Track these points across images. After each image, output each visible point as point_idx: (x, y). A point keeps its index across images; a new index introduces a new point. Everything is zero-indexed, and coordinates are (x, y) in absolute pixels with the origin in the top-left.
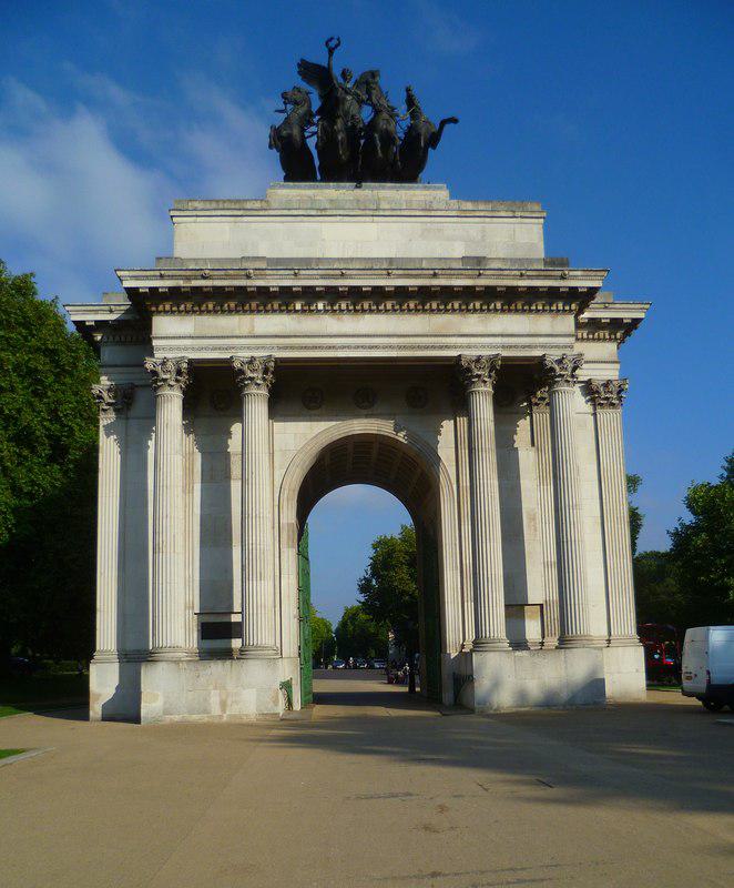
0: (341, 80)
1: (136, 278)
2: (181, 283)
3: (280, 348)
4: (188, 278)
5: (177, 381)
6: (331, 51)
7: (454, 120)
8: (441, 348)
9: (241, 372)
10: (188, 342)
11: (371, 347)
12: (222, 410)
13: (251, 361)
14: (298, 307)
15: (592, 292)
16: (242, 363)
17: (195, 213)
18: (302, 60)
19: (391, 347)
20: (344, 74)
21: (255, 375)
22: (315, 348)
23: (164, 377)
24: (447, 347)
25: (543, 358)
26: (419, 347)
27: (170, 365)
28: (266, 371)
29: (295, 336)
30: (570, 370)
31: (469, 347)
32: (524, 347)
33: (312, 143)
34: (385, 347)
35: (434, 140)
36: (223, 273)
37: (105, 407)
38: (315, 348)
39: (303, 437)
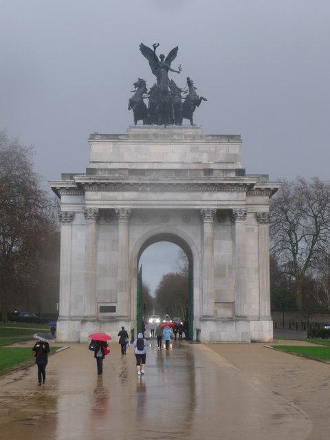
0: (160, 60)
1: (81, 179)
2: (97, 181)
4: (100, 180)
6: (155, 48)
7: (205, 100)
8: (194, 205)
10: (99, 202)
13: (123, 209)
14: (140, 189)
15: (253, 185)
19: (175, 205)
20: (162, 57)
23: (90, 215)
24: (197, 205)
25: (231, 211)
31: (204, 205)
32: (226, 205)
33: (146, 102)
35: (197, 102)
39: (140, 232)
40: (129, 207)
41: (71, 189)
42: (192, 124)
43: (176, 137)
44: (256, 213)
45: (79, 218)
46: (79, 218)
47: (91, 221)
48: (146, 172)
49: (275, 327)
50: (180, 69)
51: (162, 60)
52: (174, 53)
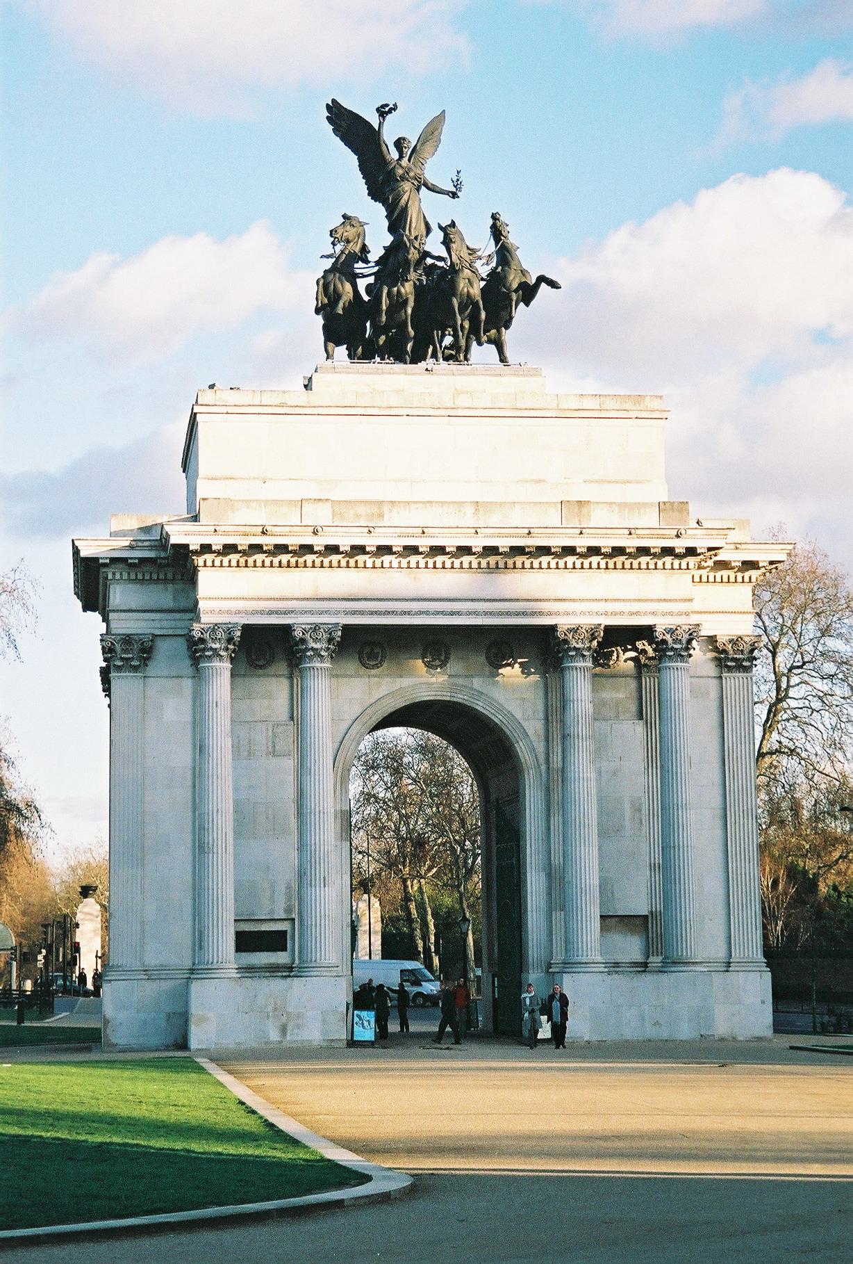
0: (394, 154)
3: (346, 613)
5: (227, 649)
9: (303, 641)
11: (452, 613)
12: (261, 667)
13: (316, 628)
16: (305, 631)
17: (224, 410)
18: (333, 101)
19: (476, 613)
21: (318, 646)
22: (387, 613)
26: (508, 614)
27: (221, 634)
28: (330, 640)
29: (366, 599)
30: (684, 642)
34: (469, 613)
35: (528, 293)
36: (288, 529)
37: (119, 663)
38: (387, 613)
40: (333, 620)
41: (143, 560)
42: (503, 359)
43: (463, 401)
44: (712, 640)
45: (169, 654)
46: (169, 654)
47: (216, 664)
48: (386, 508)
49: (779, 995)
50: (458, 184)
51: (401, 157)
52: (432, 132)
